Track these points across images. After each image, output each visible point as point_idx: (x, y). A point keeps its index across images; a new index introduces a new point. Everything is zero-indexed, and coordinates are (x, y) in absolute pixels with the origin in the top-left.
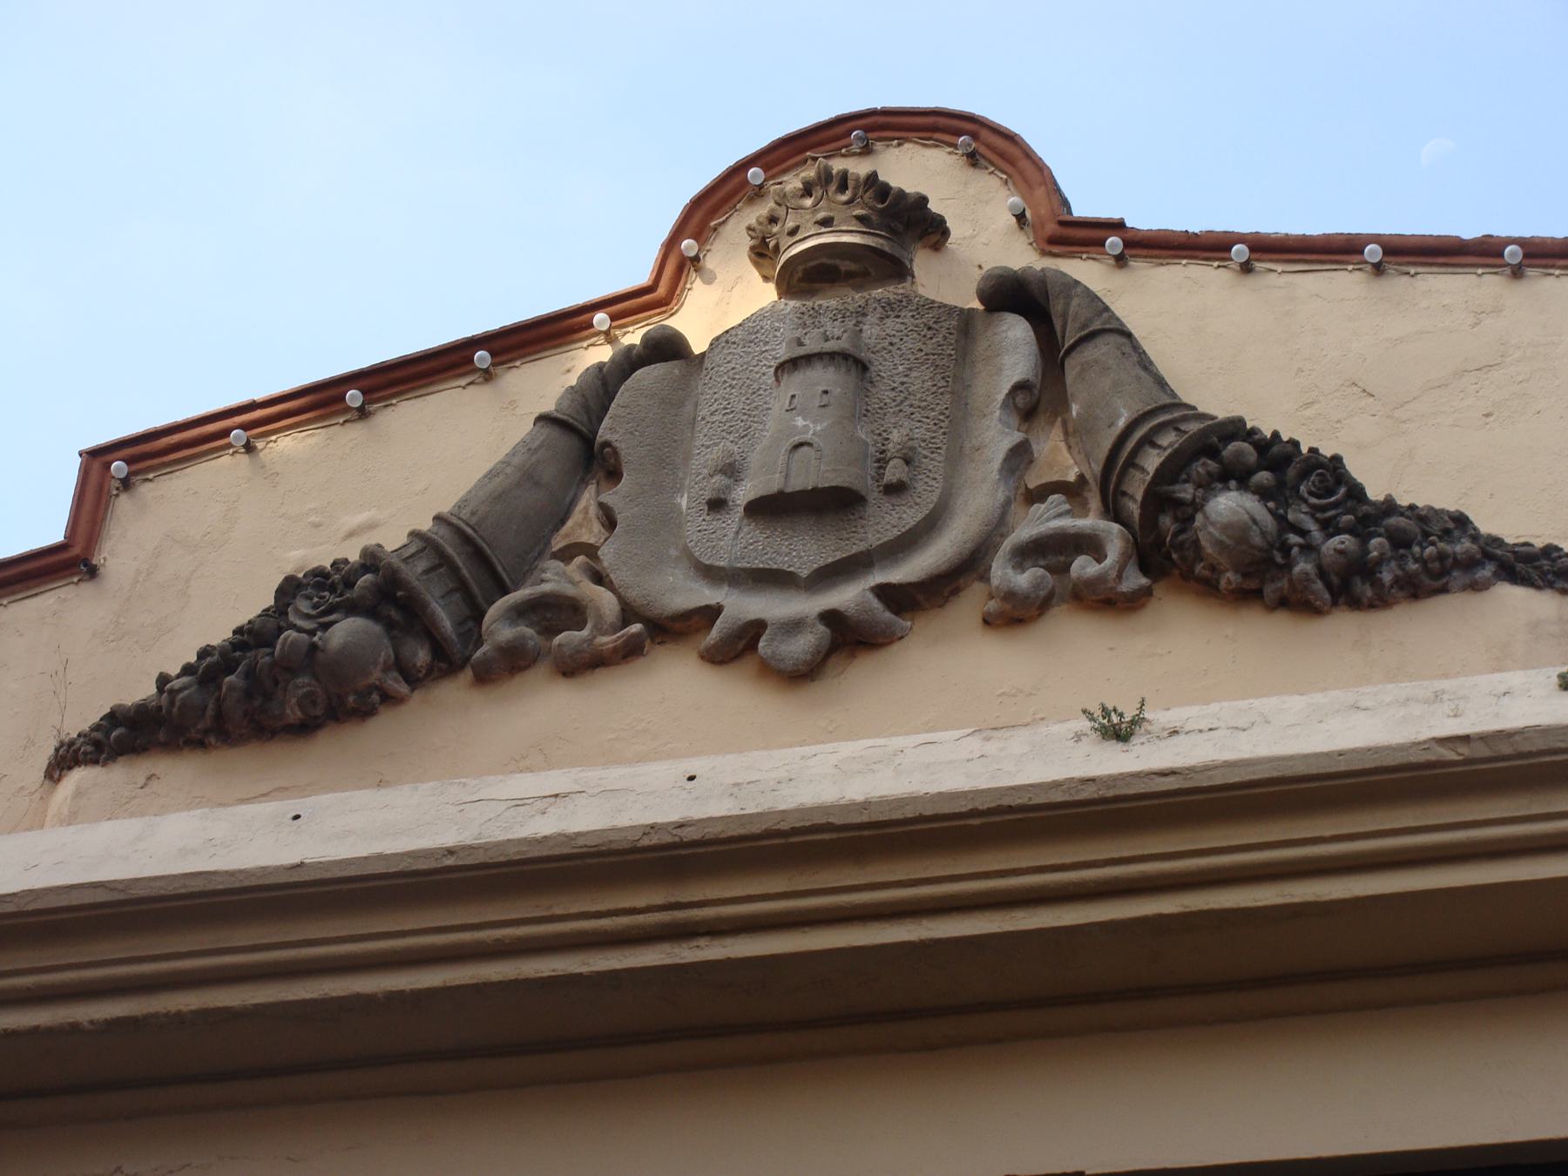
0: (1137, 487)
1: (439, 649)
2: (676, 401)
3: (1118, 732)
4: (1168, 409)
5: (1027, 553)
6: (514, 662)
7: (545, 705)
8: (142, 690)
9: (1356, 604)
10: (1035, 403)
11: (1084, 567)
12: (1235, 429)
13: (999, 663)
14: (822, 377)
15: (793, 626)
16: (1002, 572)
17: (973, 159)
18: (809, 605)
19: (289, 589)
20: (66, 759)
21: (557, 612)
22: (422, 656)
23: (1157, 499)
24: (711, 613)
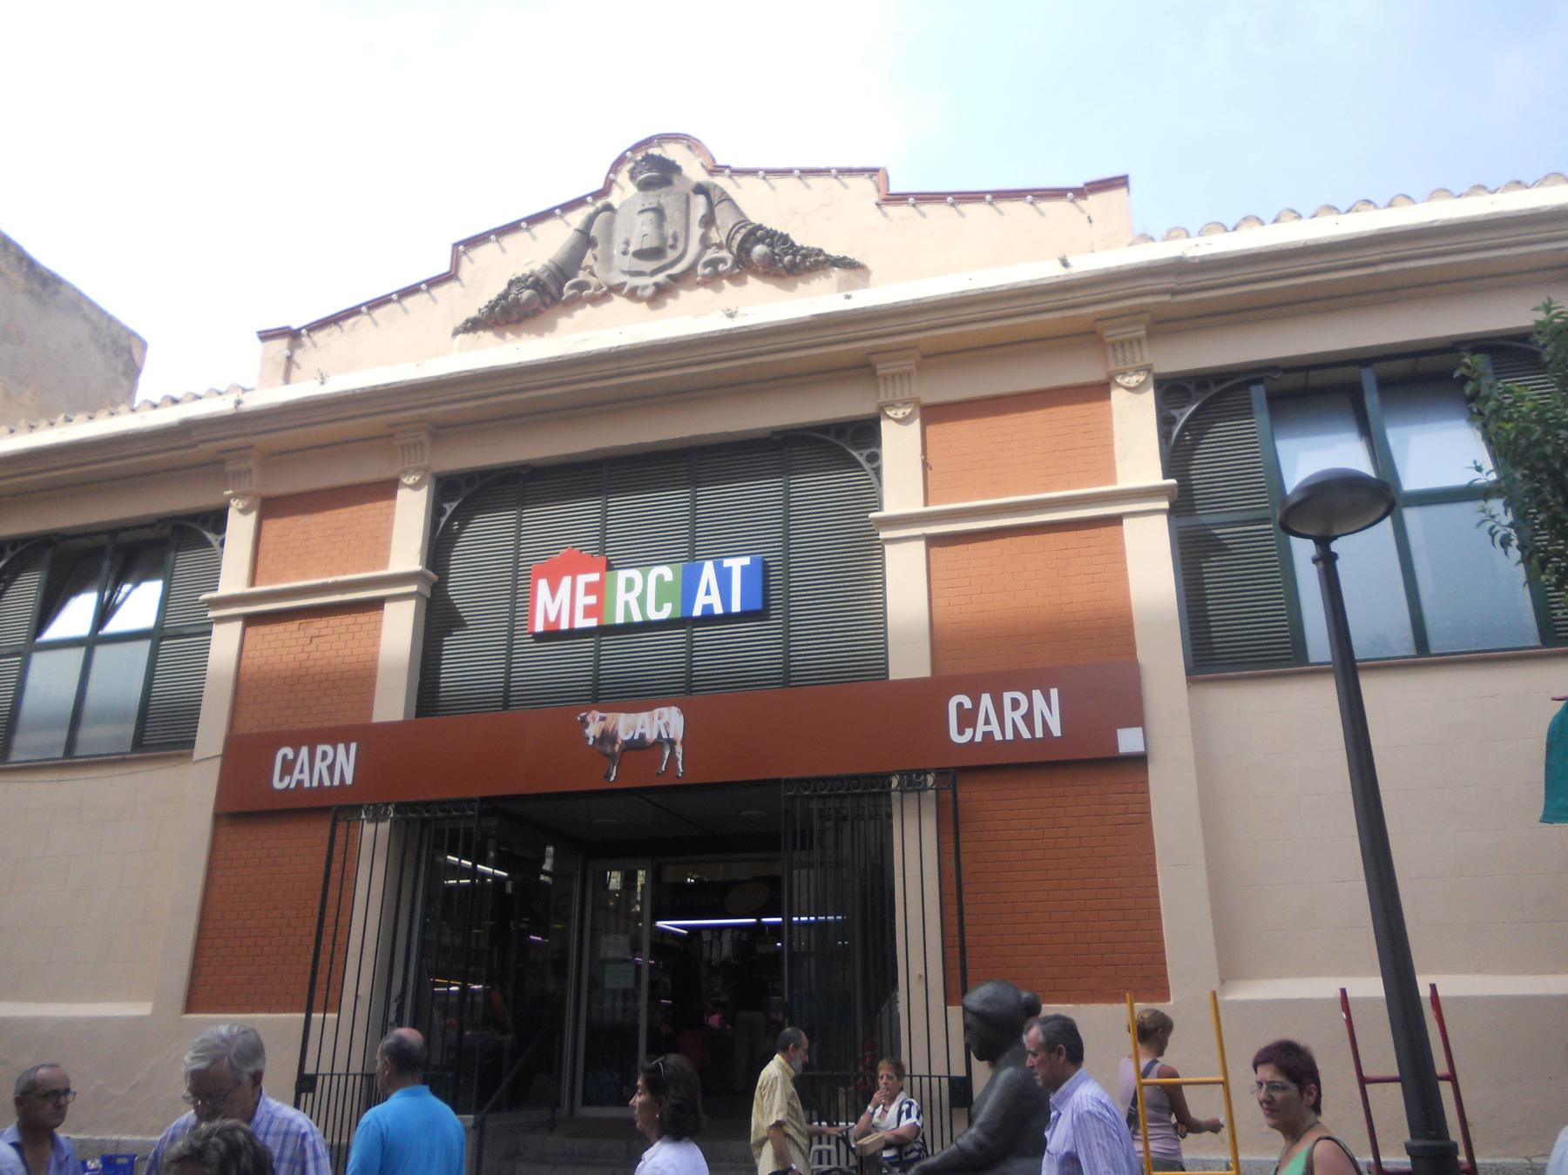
0: (735, 244)
1: (553, 298)
2: (610, 224)
3: (731, 315)
4: (744, 222)
5: (706, 265)
6: (575, 302)
7: (585, 313)
8: (474, 313)
9: (794, 274)
10: (708, 221)
11: (721, 267)
12: (760, 227)
13: (703, 294)
14: (650, 215)
15: (645, 287)
16: (700, 270)
17: (689, 147)
18: (649, 281)
19: (511, 283)
20: (456, 333)
21: (582, 286)
22: (548, 300)
23: (741, 247)
24: (624, 284)
